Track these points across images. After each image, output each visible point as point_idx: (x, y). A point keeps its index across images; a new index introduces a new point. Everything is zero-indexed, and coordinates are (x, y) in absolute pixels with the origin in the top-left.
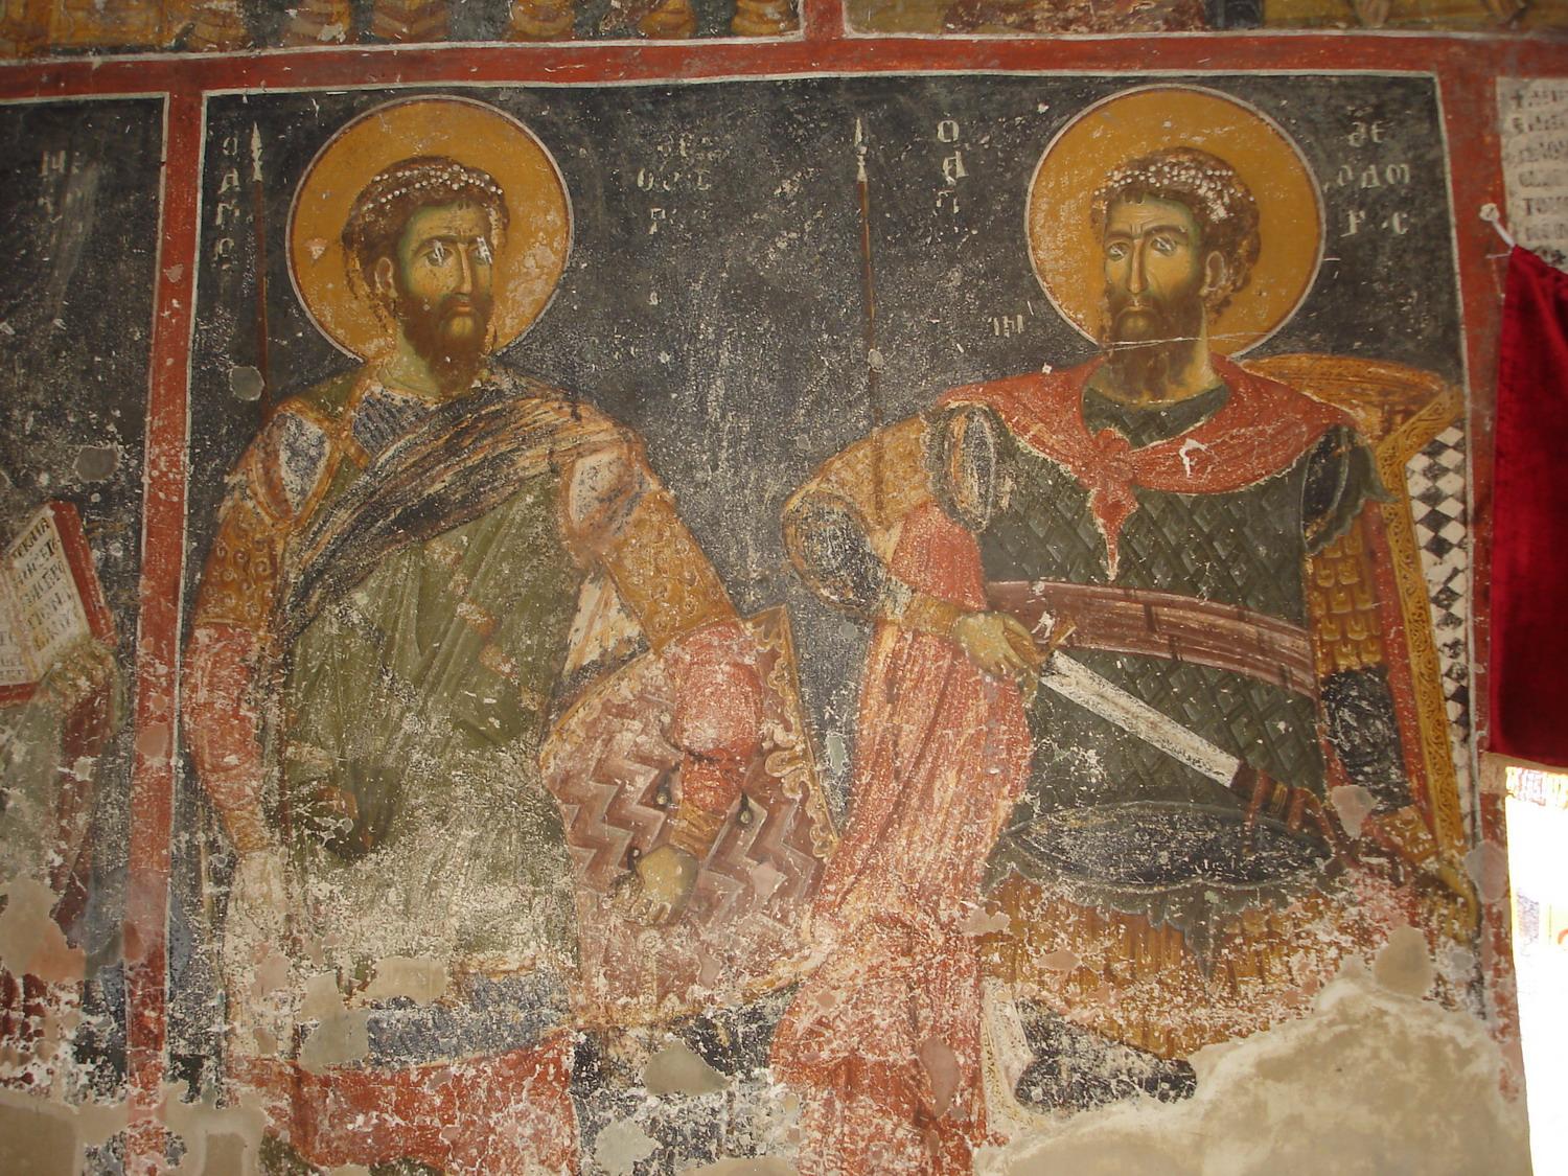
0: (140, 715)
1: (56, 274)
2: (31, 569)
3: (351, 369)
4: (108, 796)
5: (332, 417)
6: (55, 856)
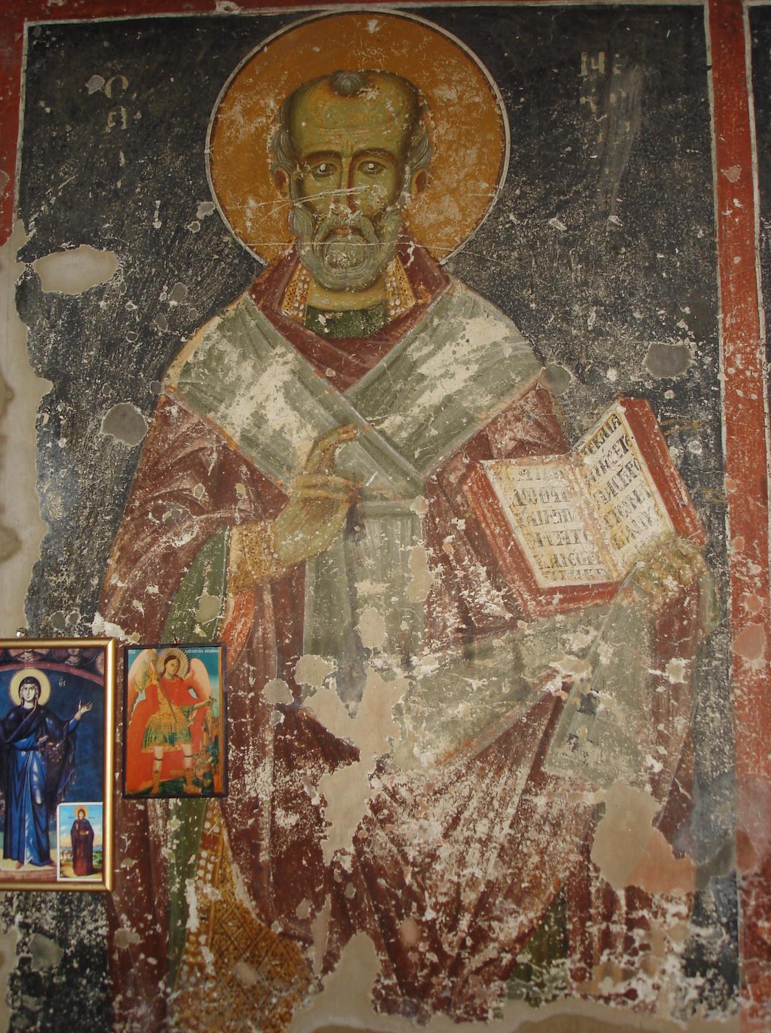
0: (735, 616)
1: (607, 171)
2: (604, 466)
4: (706, 699)
6: (654, 762)
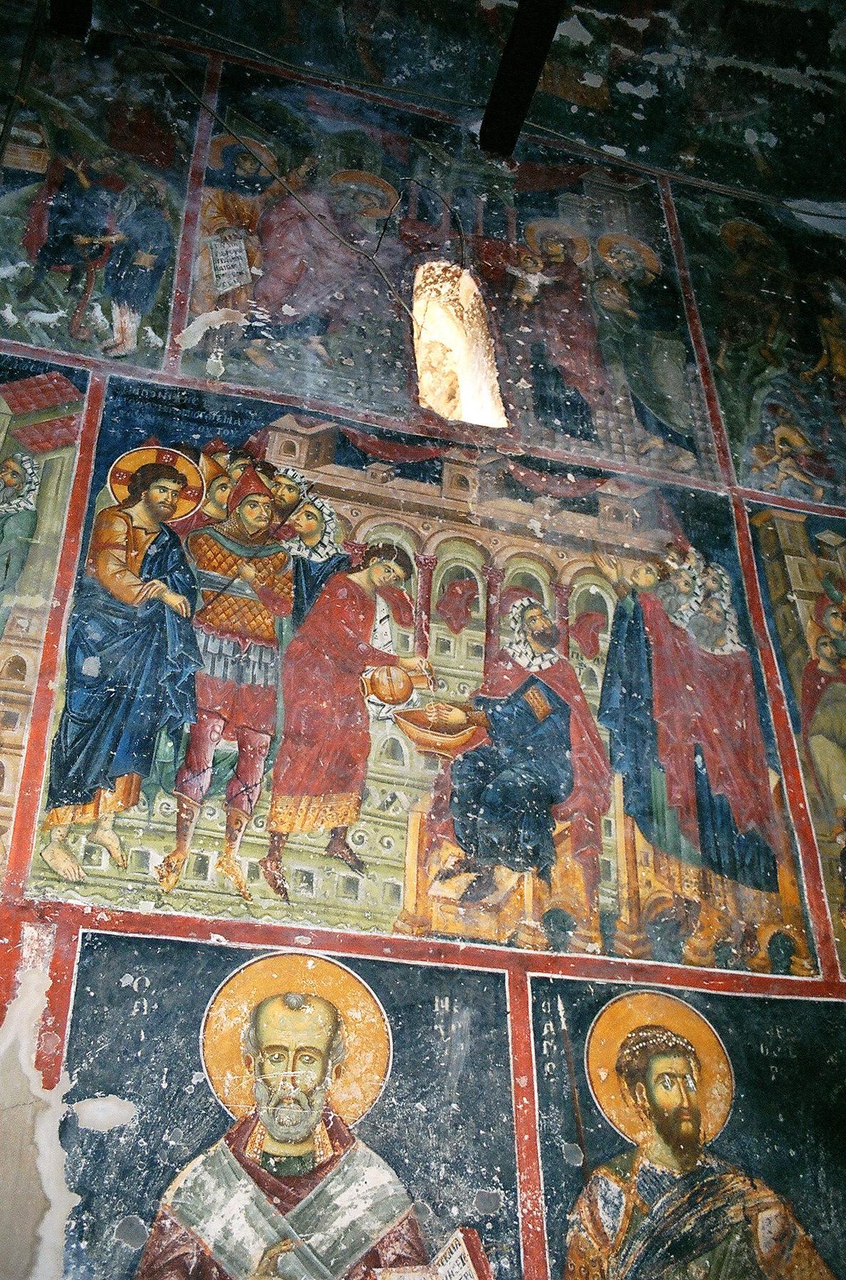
3: (631, 1149)
5: (624, 1179)
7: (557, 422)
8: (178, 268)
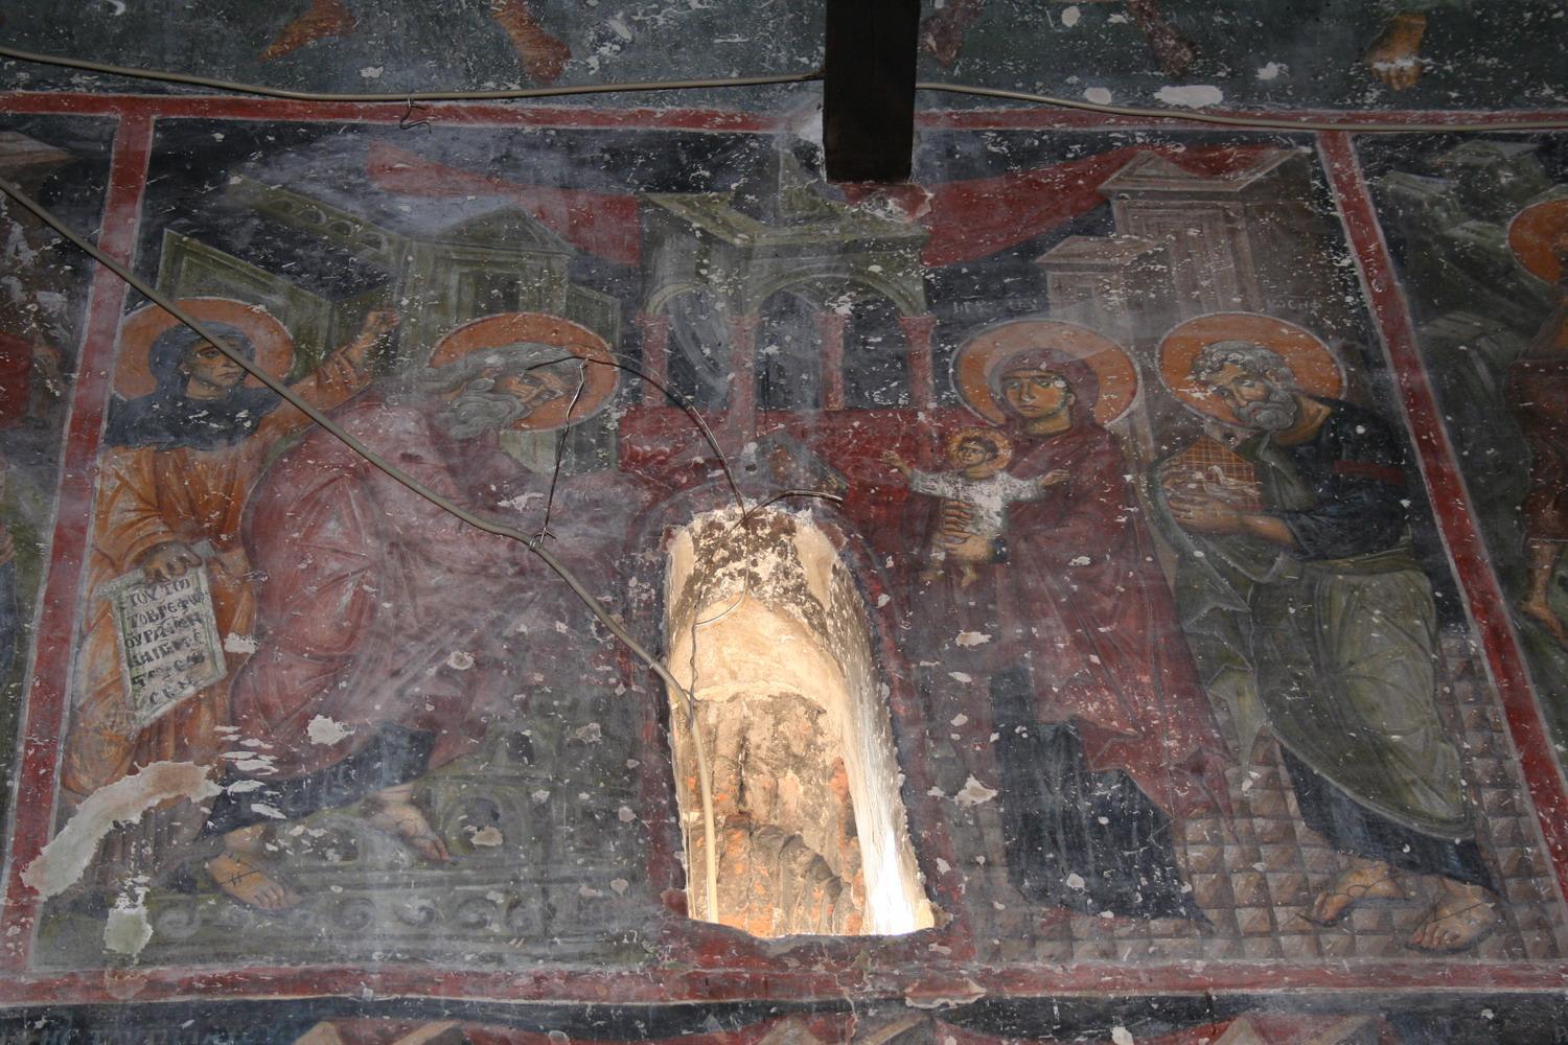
7: (1075, 881)
8: (31, 680)
